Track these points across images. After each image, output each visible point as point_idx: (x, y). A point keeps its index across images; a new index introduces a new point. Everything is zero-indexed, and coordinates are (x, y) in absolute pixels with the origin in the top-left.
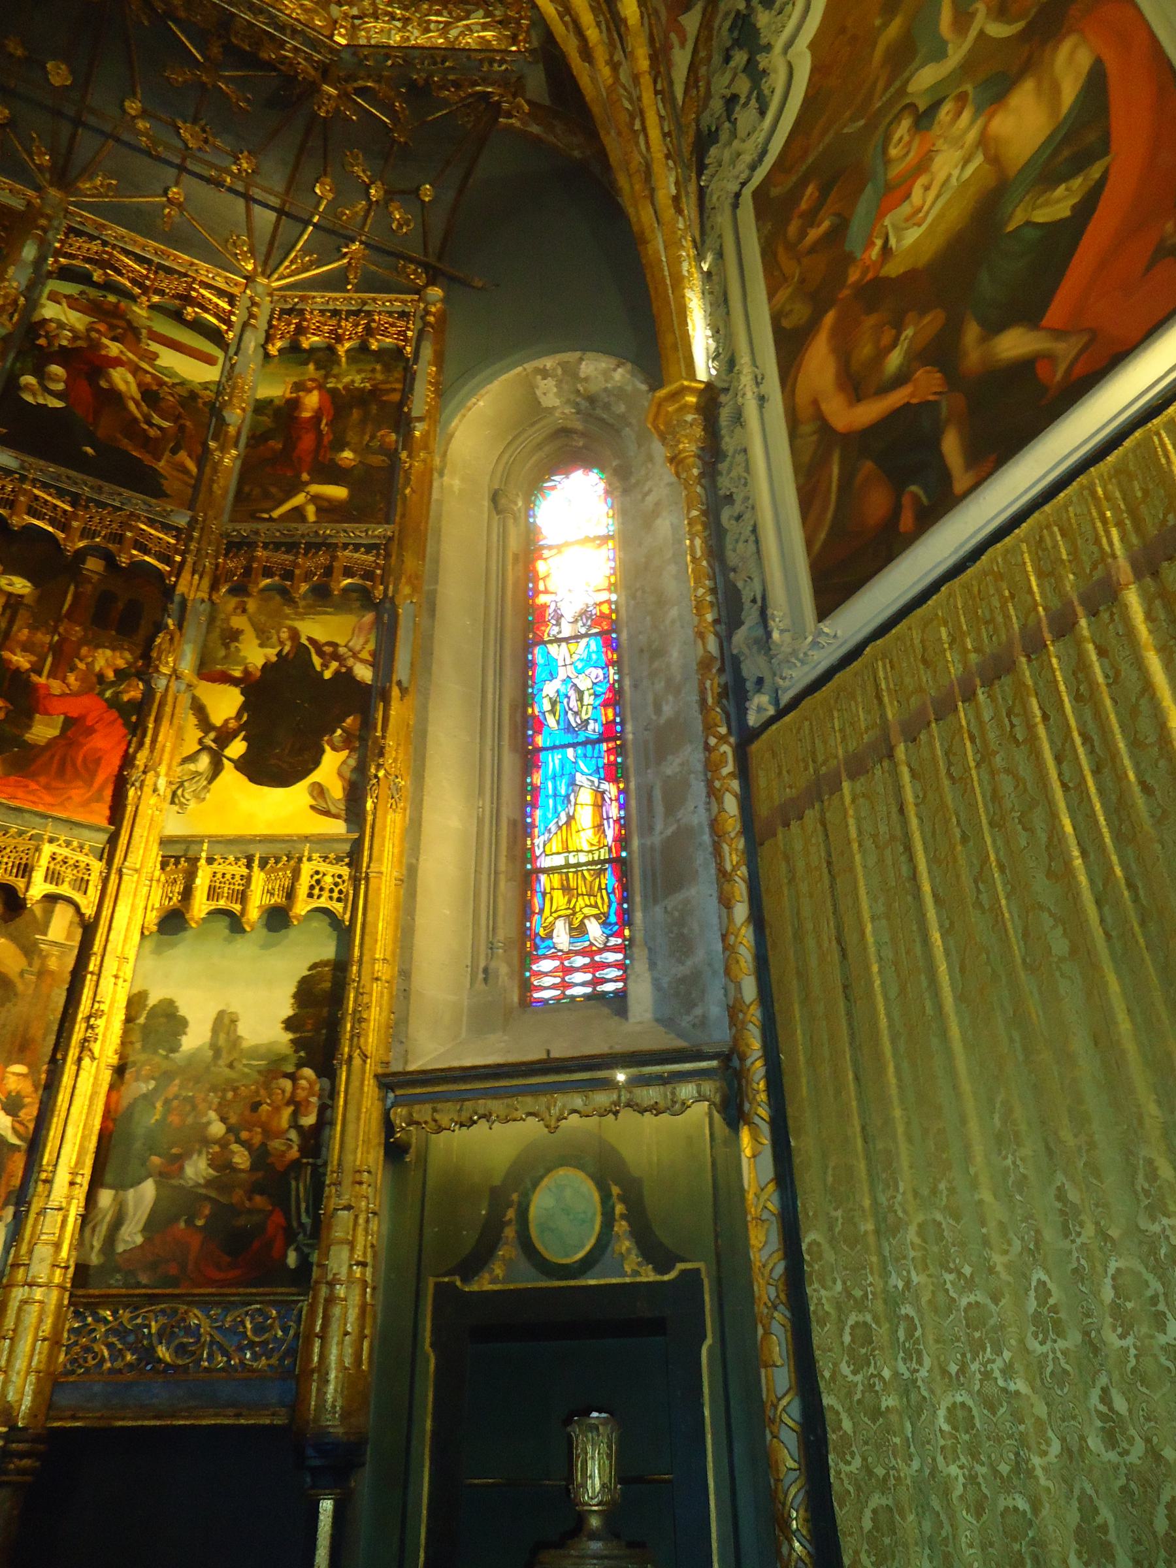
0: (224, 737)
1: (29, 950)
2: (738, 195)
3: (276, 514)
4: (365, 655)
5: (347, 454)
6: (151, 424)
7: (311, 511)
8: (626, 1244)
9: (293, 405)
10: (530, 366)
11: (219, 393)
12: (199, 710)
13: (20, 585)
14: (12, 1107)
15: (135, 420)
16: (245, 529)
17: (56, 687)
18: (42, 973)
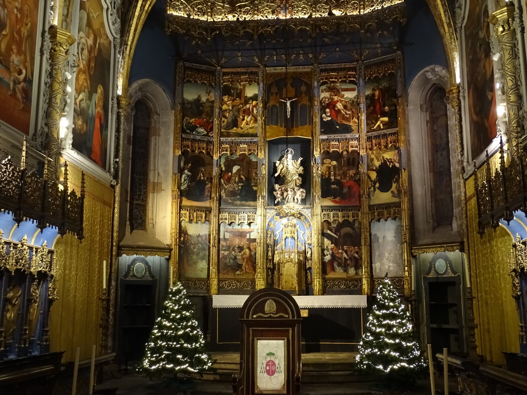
0: (375, 184)
1: (353, 229)
2: (461, 26)
3: (375, 128)
4: (397, 161)
5: (387, 108)
6: (347, 114)
7: (381, 125)
8: (450, 271)
9: (373, 95)
10: (423, 70)
11: (358, 99)
12: (369, 177)
13: (334, 163)
14: (357, 253)
15: (344, 115)
16: (370, 134)
17: (345, 181)
18: (356, 232)
